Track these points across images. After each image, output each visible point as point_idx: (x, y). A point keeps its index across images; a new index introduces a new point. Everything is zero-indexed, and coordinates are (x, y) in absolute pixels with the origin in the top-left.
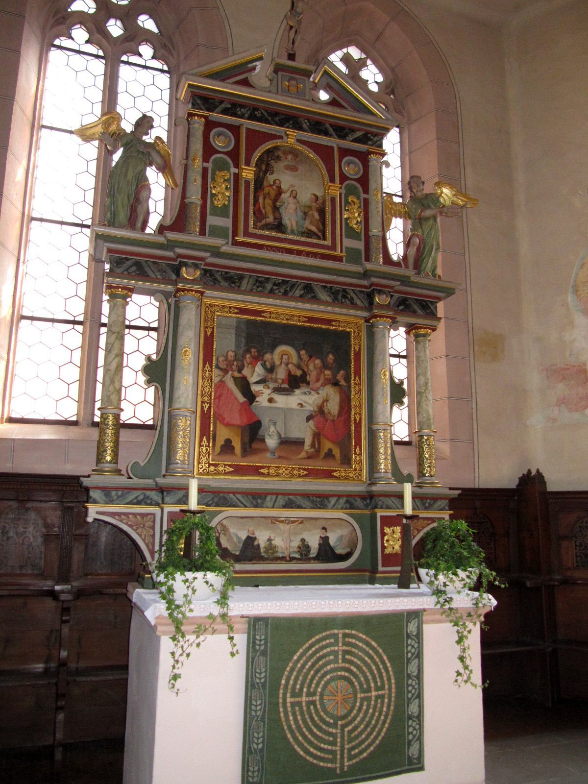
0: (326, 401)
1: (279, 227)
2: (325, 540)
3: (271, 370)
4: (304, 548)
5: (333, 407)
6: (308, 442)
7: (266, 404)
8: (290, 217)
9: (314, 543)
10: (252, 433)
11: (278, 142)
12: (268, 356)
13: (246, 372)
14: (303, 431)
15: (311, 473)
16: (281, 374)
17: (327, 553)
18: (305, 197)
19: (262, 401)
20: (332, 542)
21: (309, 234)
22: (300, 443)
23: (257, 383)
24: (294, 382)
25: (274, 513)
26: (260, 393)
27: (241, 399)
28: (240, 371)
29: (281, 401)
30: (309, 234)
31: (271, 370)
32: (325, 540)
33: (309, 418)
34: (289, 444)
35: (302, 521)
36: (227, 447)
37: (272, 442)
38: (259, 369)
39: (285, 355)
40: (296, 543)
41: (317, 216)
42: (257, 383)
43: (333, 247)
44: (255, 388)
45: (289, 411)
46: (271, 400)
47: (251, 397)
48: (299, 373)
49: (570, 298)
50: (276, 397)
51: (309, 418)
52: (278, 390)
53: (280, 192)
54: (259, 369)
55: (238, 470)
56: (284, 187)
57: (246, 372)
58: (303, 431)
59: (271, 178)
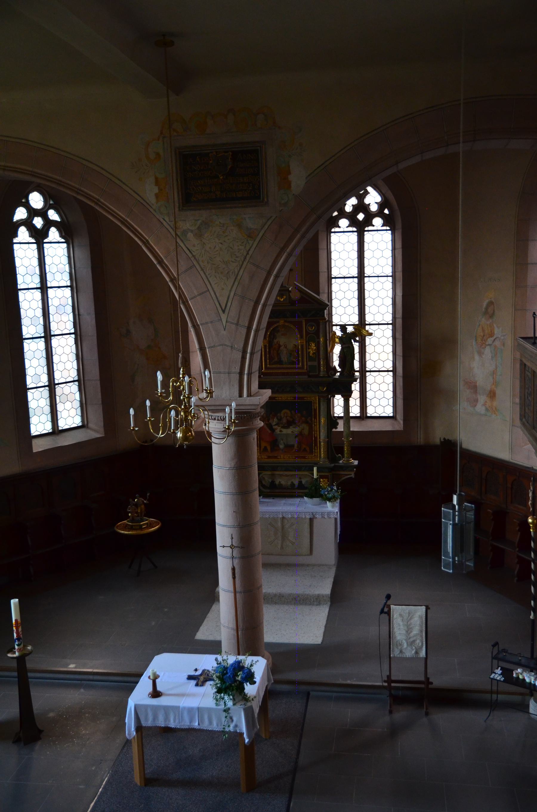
0: (303, 429)
1: (280, 362)
2: (300, 482)
3: (280, 419)
4: (293, 485)
5: (306, 432)
6: (296, 445)
7: (279, 432)
8: (284, 357)
9: (296, 482)
10: (274, 444)
11: (278, 324)
12: (279, 414)
13: (271, 421)
14: (293, 441)
15: (296, 457)
16: (284, 421)
17: (301, 486)
18: (290, 347)
19: (278, 431)
20: (303, 482)
21: (293, 363)
22: (293, 446)
23: (275, 425)
24: (289, 424)
25: (281, 473)
26: (276, 429)
27: (270, 432)
28: (268, 421)
29: (285, 431)
30: (293, 363)
31: (280, 419)
32: (300, 482)
33: (296, 437)
34: (289, 447)
35: (292, 475)
36: (265, 449)
37: (281, 446)
38: (275, 420)
39: (285, 413)
40: (289, 483)
41: (296, 354)
42: (275, 425)
43: (302, 367)
44: (274, 427)
45: (289, 434)
46: (281, 431)
47: (273, 430)
48: (291, 420)
49: (474, 343)
50: (282, 430)
51: (296, 437)
52: (284, 427)
53: (280, 346)
54: (275, 420)
55: (269, 457)
56: (281, 344)
57: (271, 421)
58: (293, 441)
59: (275, 341)
